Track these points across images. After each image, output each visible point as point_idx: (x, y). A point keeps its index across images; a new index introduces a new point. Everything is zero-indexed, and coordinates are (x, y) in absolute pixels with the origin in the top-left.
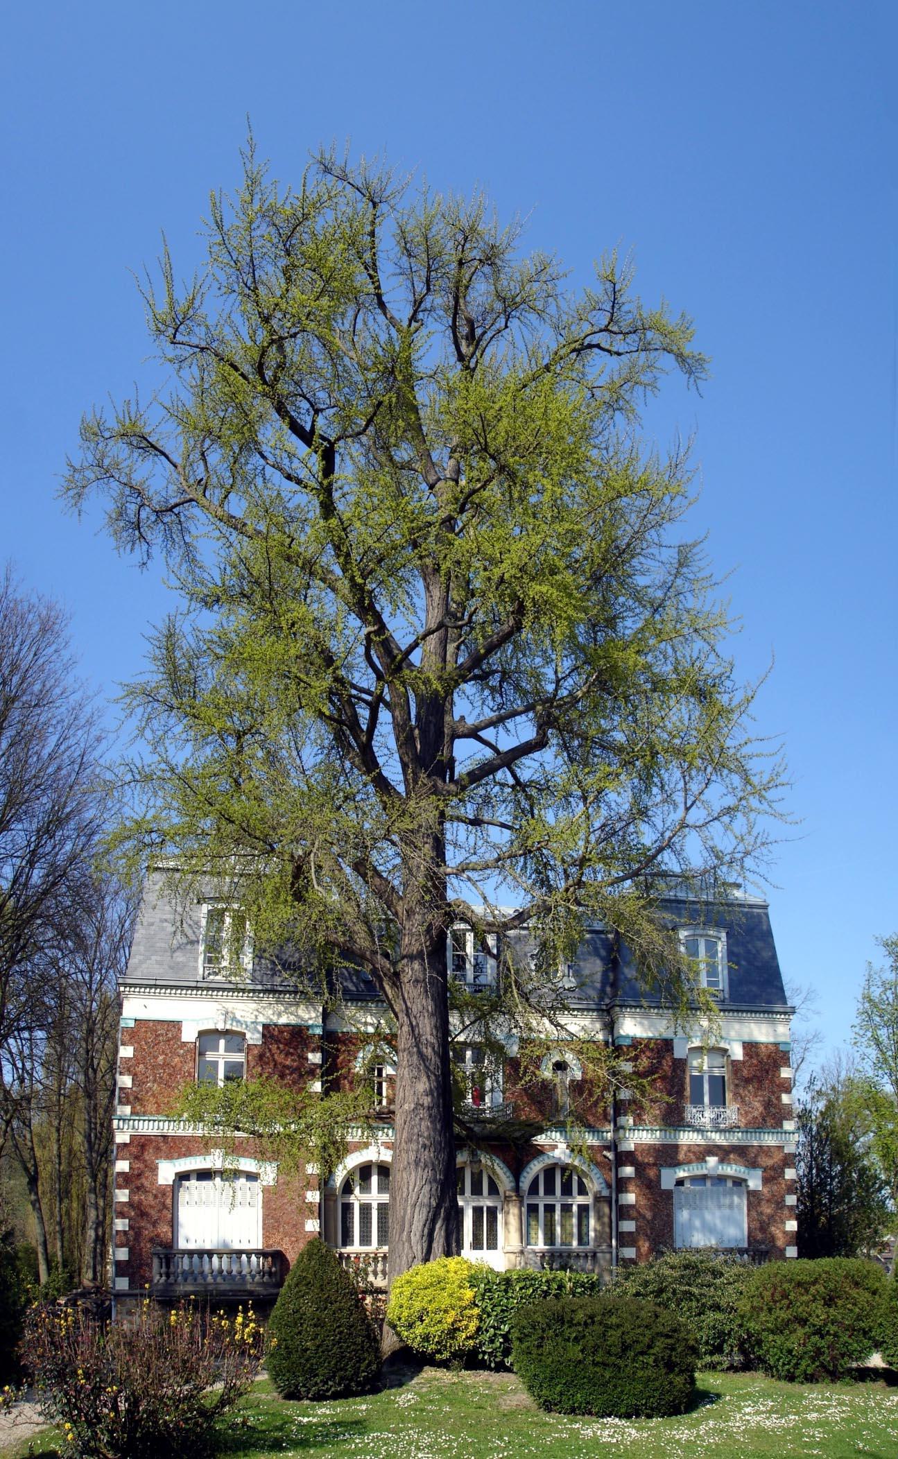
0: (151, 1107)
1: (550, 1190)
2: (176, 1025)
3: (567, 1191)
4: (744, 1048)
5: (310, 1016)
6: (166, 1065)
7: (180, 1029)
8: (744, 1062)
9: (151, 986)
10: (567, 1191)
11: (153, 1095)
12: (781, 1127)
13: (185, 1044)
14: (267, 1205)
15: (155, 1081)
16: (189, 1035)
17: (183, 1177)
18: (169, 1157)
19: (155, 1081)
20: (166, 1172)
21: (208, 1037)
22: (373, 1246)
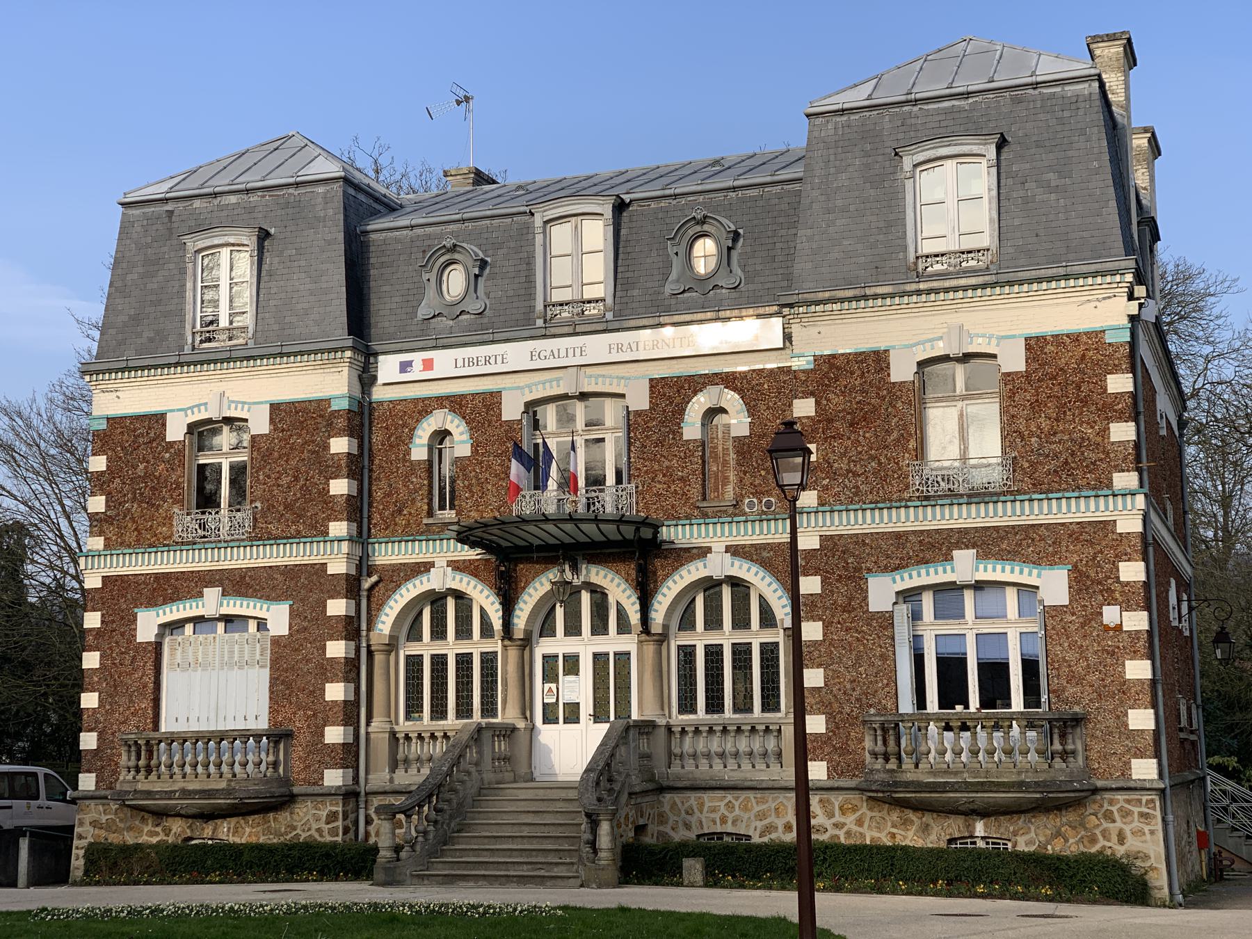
0: (131, 537)
1: (713, 622)
2: (158, 420)
3: (741, 622)
4: (1029, 348)
5: (329, 383)
6: (147, 475)
7: (164, 425)
8: (1027, 375)
9: (123, 370)
10: (741, 622)
11: (133, 519)
12: (1110, 485)
13: (171, 444)
14: (276, 665)
15: (134, 499)
16: (175, 431)
17: (174, 626)
18: (152, 603)
19: (134, 499)
20: (147, 624)
21: (202, 432)
22: (451, 721)
